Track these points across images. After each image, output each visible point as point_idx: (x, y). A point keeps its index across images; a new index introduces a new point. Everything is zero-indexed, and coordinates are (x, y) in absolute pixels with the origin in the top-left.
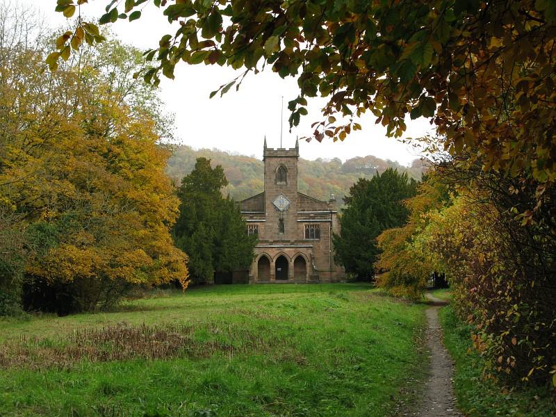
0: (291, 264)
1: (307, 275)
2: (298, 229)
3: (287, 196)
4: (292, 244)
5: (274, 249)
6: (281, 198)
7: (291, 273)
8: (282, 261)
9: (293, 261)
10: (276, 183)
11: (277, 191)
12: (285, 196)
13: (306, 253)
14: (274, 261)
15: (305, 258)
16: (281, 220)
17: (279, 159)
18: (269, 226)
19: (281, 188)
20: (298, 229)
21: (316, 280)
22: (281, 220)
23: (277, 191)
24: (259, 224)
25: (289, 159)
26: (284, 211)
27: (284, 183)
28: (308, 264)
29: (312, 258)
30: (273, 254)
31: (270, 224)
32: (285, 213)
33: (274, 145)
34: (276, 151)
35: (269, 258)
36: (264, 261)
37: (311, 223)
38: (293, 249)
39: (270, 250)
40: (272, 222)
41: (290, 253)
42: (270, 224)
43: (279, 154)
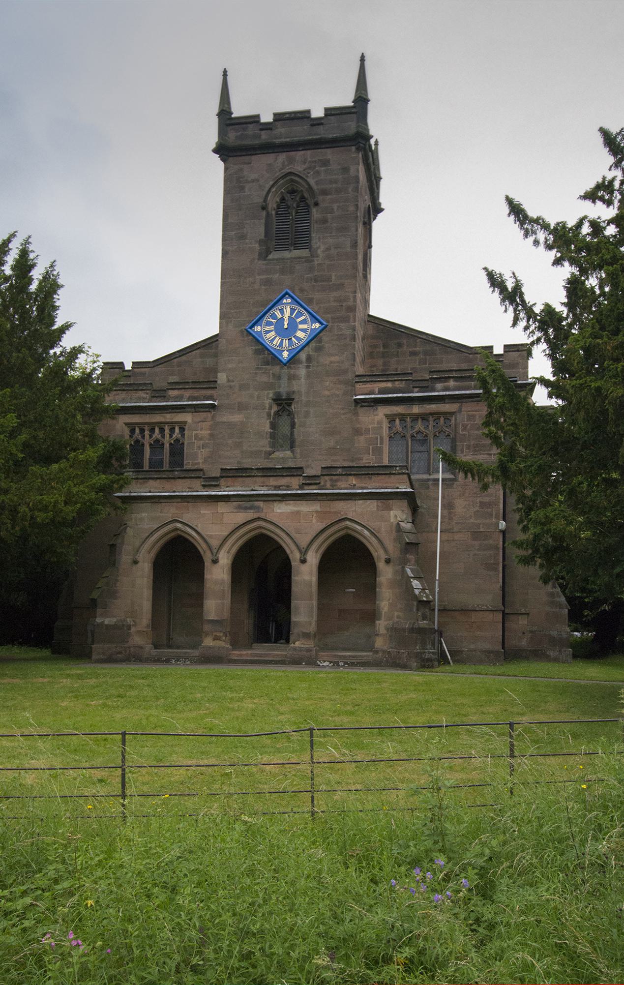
0: (305, 574)
1: (382, 625)
2: (357, 432)
3: (310, 301)
4: (312, 480)
5: (222, 507)
6: (286, 311)
7: (304, 612)
8: (263, 568)
9: (313, 559)
10: (264, 255)
11: (268, 282)
12: (303, 302)
13: (380, 525)
14: (225, 559)
15: (379, 554)
16: (284, 404)
17: (282, 157)
18: (230, 425)
19: (283, 272)
20: (357, 432)
21: (427, 644)
22: (284, 404)
23: (268, 282)
24: (187, 417)
25: (328, 154)
26: (293, 360)
27: (305, 253)
28: (386, 574)
29: (412, 548)
30: (217, 530)
31: (237, 418)
32: (302, 372)
33: (258, 101)
34: (267, 127)
35: (202, 547)
36: (179, 560)
37: (416, 409)
38: (316, 506)
39: (206, 511)
40: (241, 407)
41: (300, 526)
42: (237, 418)
43: (283, 134)
